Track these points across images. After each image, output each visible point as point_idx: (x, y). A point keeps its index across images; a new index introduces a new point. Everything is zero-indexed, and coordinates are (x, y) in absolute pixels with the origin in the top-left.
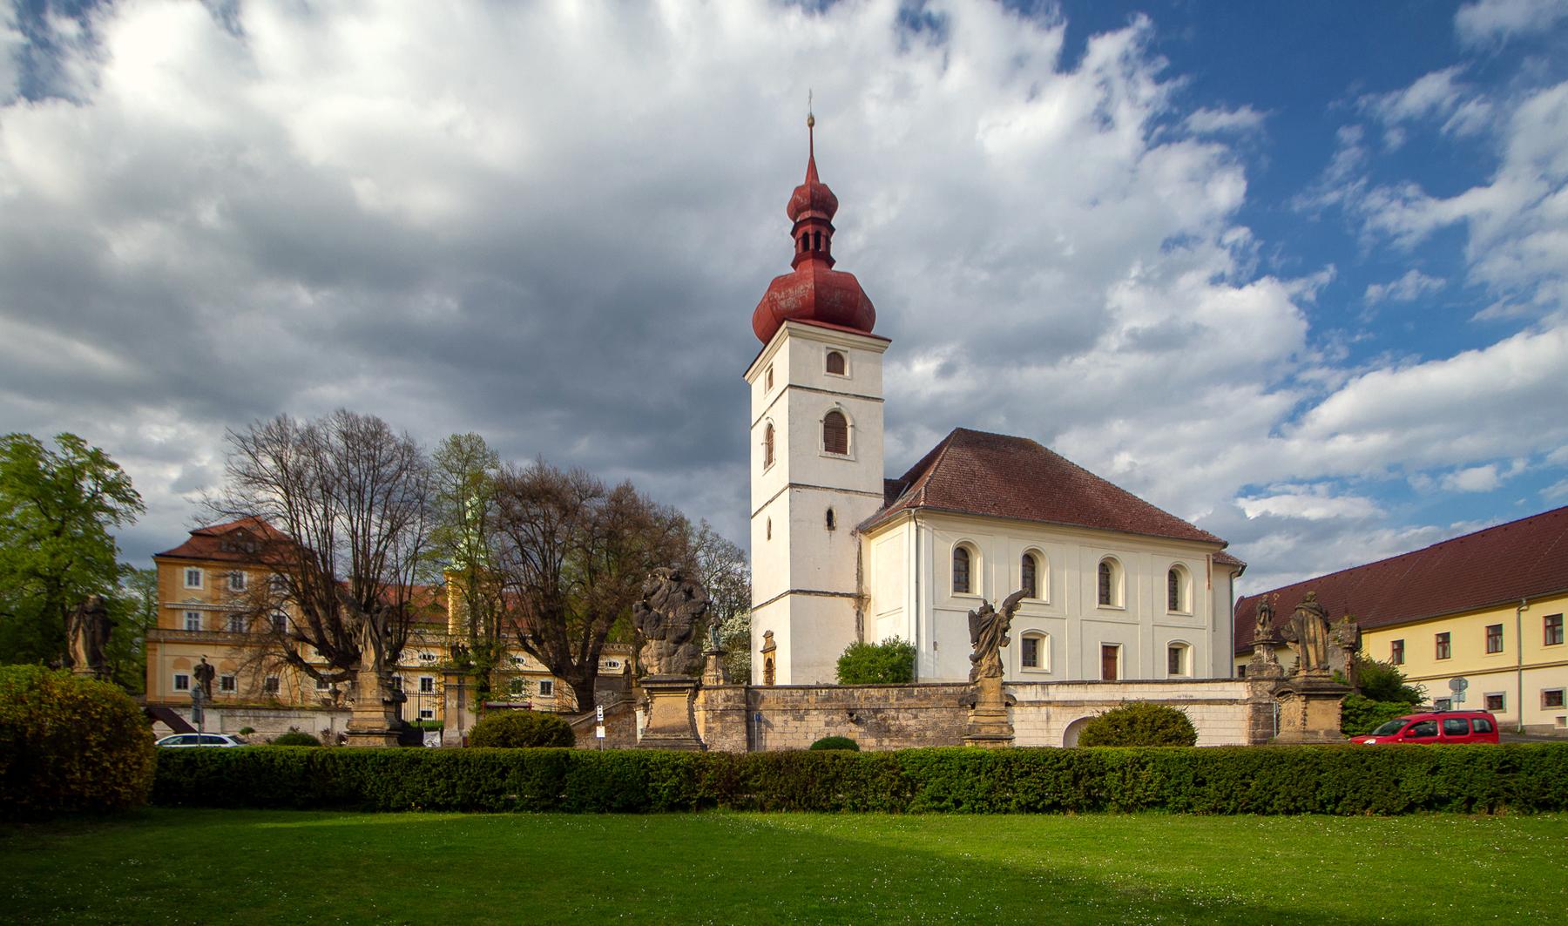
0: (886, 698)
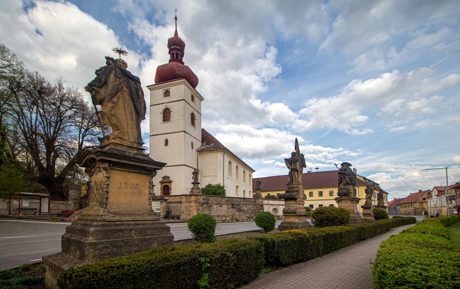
0: (240, 201)
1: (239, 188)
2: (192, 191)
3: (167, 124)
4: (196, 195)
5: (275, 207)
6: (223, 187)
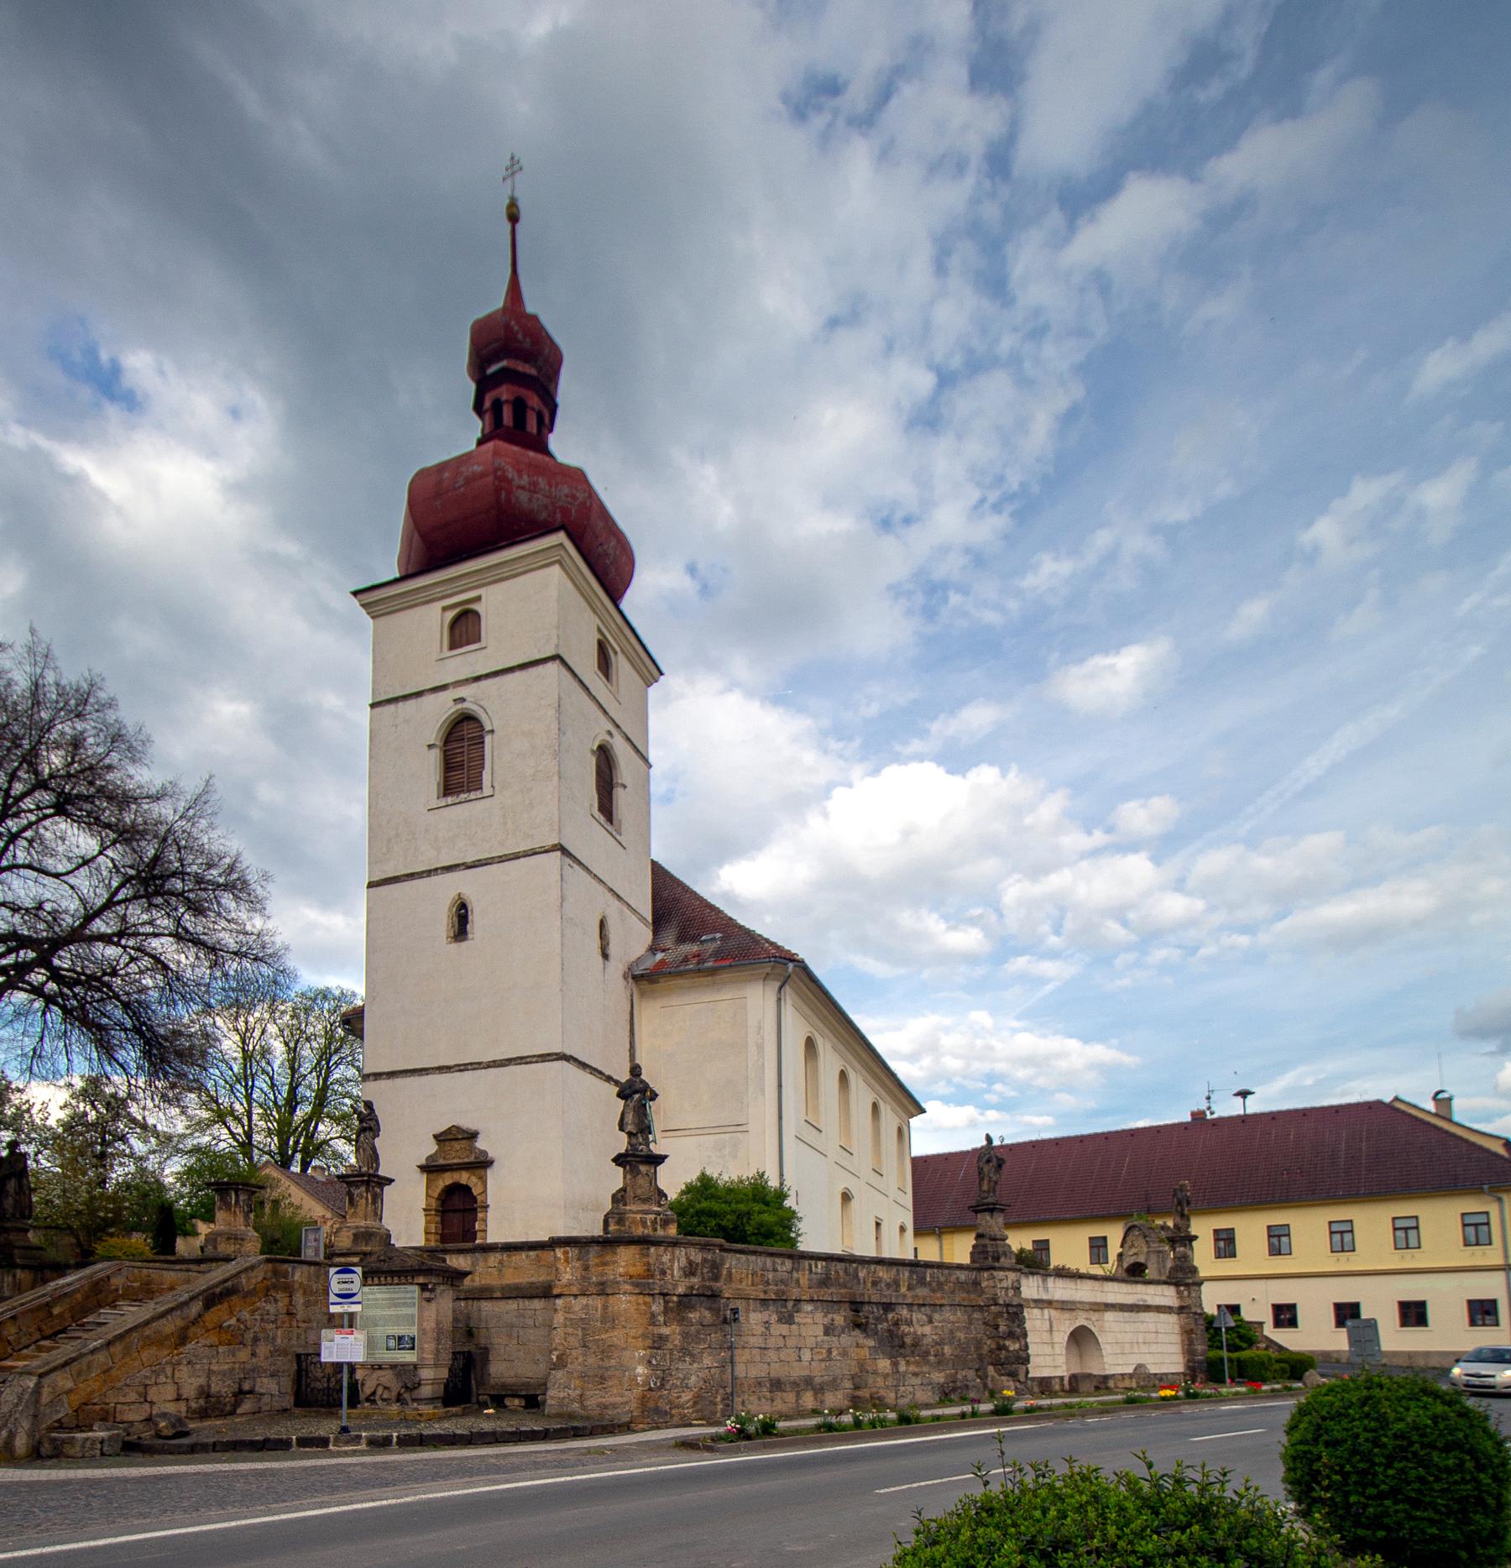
1: (854, 1203)
2: (615, 1215)
3: (464, 811)
4: (645, 1242)
5: (1081, 1320)
6: (781, 1195)
